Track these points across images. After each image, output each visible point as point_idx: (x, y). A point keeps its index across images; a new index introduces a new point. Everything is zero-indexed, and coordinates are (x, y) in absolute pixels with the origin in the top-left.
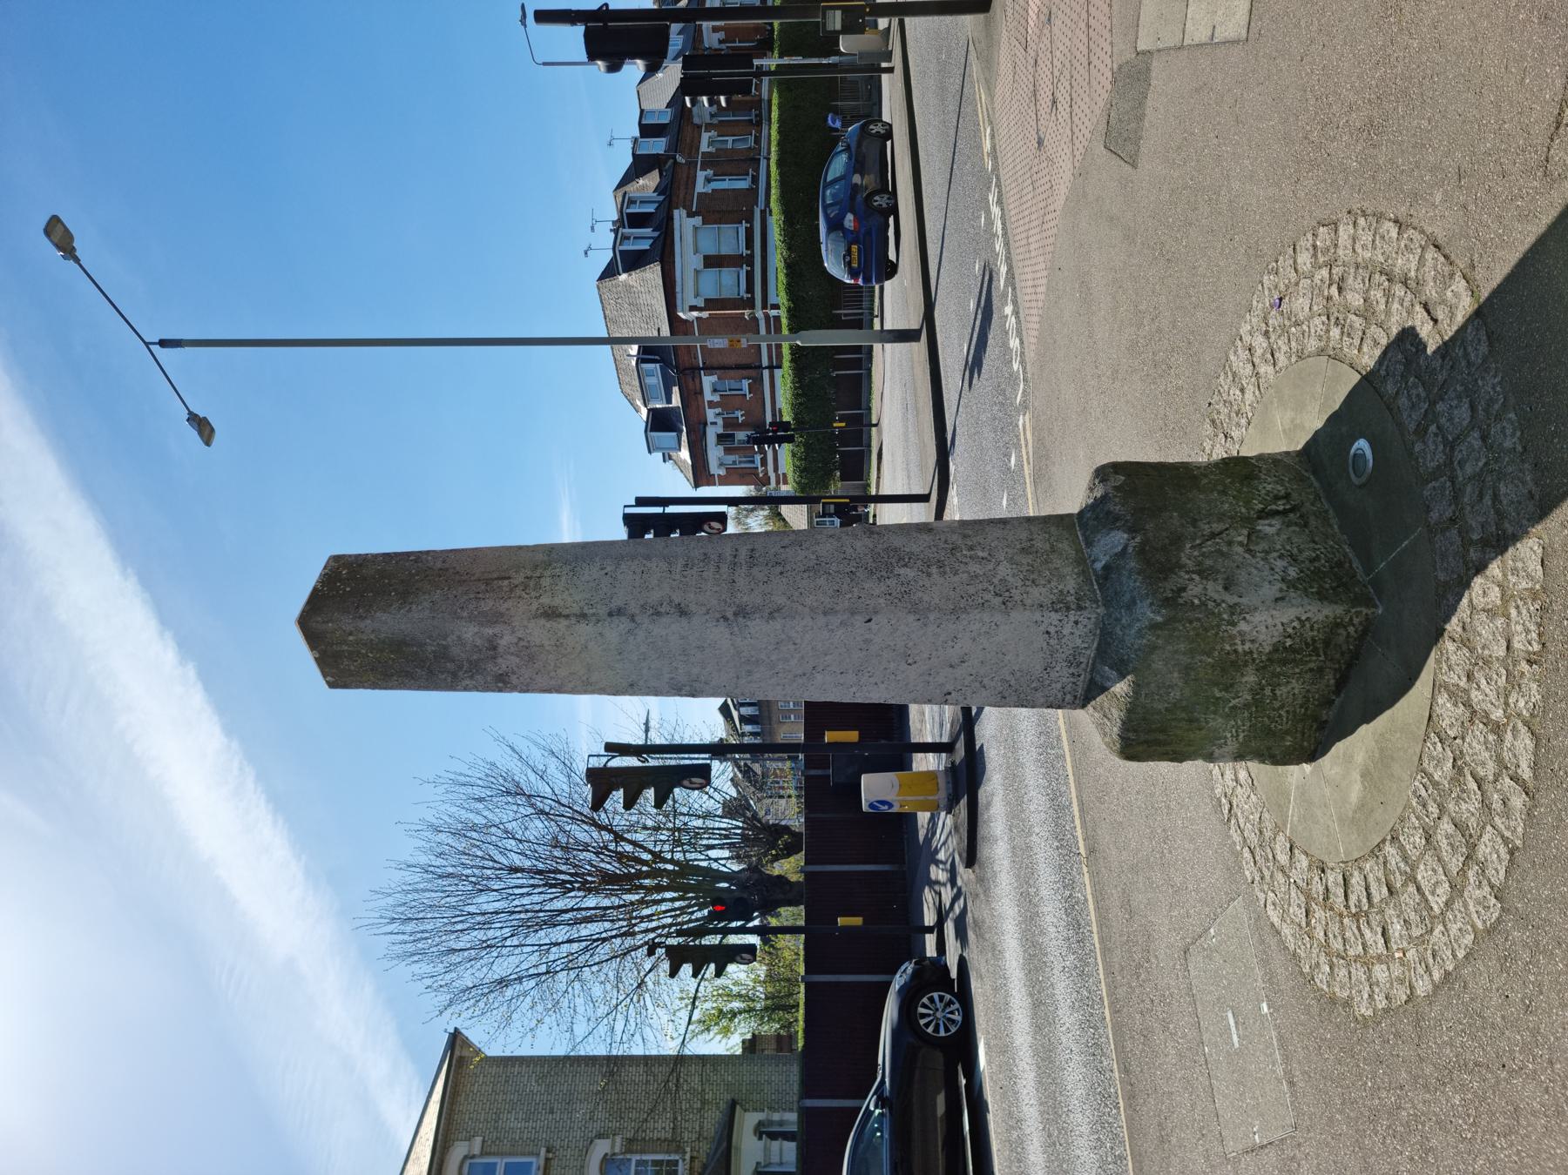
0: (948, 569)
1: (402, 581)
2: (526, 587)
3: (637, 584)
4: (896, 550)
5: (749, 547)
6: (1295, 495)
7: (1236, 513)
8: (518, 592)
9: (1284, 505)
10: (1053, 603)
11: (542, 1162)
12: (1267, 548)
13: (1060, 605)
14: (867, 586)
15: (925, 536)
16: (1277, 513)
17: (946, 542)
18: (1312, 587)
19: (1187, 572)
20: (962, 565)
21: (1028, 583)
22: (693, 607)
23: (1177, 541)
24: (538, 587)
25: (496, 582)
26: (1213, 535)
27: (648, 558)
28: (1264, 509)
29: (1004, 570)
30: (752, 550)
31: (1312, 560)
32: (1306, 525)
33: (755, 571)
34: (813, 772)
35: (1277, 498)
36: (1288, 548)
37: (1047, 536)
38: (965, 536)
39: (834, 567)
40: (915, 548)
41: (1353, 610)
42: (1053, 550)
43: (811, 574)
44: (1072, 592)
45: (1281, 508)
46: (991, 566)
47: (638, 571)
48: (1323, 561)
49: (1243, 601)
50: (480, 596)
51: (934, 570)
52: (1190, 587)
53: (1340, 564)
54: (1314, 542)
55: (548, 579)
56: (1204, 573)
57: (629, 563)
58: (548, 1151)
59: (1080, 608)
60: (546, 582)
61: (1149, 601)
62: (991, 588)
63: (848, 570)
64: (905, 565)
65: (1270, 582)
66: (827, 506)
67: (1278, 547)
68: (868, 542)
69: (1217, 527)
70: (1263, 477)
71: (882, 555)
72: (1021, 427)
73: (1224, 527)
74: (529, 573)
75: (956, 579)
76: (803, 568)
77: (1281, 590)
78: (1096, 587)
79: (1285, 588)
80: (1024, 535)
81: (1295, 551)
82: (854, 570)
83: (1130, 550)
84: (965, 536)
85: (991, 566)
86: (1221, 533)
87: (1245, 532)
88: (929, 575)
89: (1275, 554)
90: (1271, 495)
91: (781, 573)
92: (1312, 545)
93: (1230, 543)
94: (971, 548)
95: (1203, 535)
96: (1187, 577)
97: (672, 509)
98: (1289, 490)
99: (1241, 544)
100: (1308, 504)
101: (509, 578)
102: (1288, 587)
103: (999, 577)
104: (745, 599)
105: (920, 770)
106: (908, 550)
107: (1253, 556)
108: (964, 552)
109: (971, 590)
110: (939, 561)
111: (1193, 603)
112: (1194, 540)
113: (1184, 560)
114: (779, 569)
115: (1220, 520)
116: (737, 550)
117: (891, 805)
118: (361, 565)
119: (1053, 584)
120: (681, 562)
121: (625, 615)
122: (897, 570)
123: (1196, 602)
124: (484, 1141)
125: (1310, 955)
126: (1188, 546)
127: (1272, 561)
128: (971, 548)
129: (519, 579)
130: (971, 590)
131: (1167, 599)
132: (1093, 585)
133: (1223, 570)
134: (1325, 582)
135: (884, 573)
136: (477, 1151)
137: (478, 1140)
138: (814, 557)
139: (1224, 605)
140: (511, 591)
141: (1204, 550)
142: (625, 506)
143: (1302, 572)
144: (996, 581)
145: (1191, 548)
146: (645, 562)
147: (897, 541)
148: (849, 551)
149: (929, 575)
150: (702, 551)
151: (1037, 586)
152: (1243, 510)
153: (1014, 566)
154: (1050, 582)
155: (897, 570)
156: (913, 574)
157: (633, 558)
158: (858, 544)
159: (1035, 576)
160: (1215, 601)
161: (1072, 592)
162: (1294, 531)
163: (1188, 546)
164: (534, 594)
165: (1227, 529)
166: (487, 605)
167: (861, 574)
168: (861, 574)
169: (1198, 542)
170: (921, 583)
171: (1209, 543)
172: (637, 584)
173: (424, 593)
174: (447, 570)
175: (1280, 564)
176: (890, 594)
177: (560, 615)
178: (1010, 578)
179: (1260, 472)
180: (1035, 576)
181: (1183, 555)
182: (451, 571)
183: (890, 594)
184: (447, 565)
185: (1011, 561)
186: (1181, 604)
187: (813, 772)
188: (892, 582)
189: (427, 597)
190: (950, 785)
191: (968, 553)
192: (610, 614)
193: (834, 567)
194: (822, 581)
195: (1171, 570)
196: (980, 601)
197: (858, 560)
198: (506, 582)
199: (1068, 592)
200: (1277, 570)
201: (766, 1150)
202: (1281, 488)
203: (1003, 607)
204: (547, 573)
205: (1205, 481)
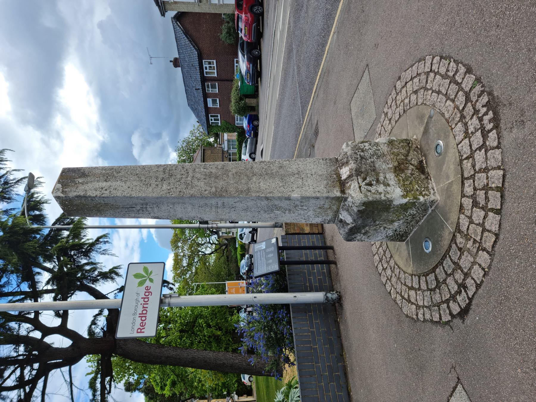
0: (292, 212)
4: (275, 205)
8: (141, 212)
17: (294, 204)
27: (184, 203)
30: (223, 203)
33: (225, 209)
39: (253, 209)
40: (282, 205)
46: (306, 212)
51: (287, 212)
70: (414, 208)
75: (294, 214)
80: (322, 203)
84: (301, 202)
104: (223, 217)
109: (297, 218)
114: (233, 209)
116: (217, 203)
122: (275, 211)
128: (302, 206)
129: (138, 207)
135: (270, 212)
147: (276, 203)
148: (259, 205)
149: (285, 213)
155: (275, 211)
157: (179, 204)
158: (262, 203)
167: (262, 212)
168: (262, 212)
185: (314, 210)
188: (272, 215)
191: (300, 207)
193: (253, 209)
194: (249, 213)
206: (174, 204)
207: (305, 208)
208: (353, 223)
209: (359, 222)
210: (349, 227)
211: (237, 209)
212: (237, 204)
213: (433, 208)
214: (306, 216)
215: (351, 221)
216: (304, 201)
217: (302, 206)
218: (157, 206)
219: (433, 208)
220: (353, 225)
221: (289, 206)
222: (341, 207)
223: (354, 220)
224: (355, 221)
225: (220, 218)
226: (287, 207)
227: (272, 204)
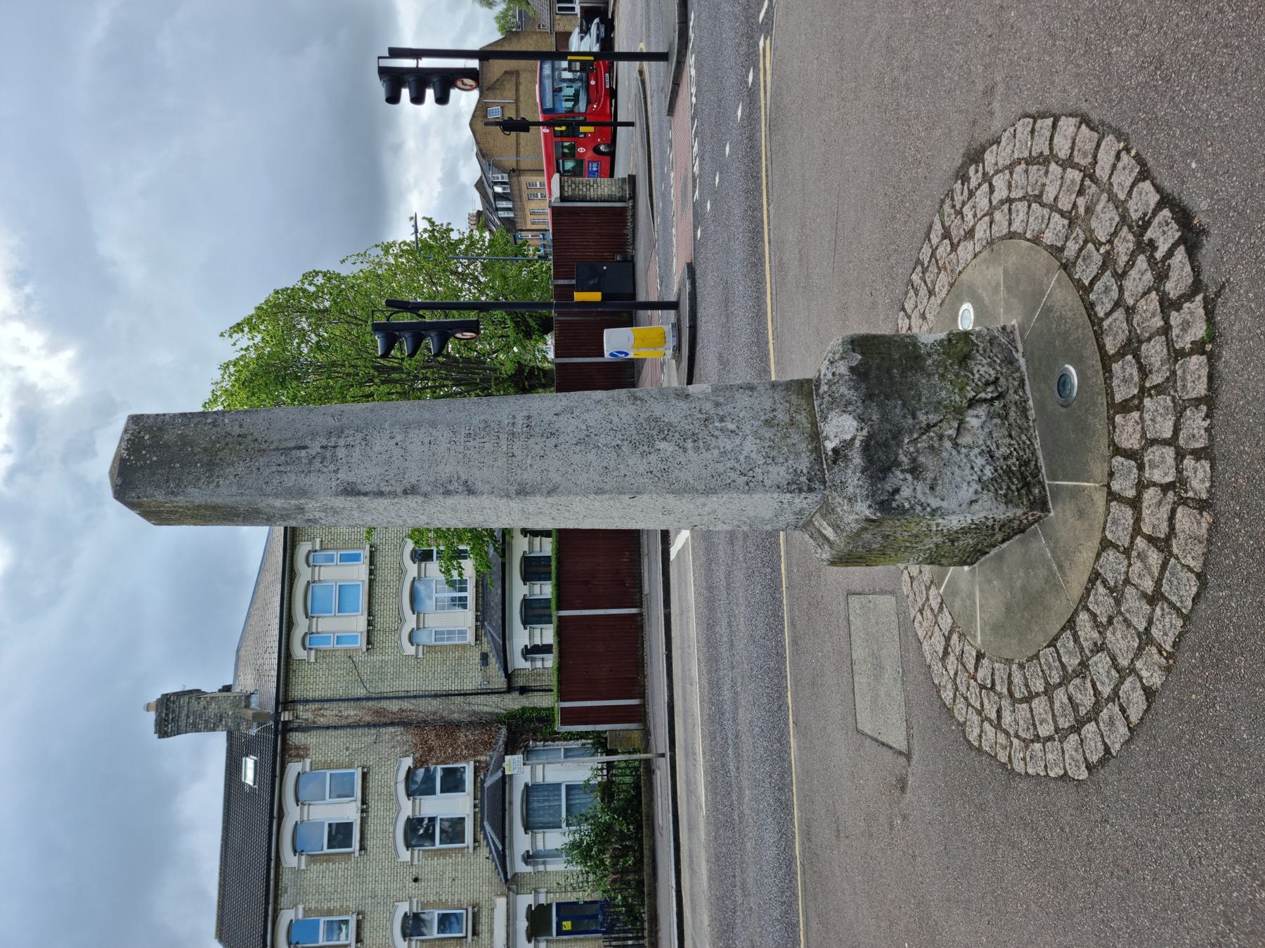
0: (701, 444)
1: (205, 450)
2: (324, 459)
3: (426, 458)
4: (656, 420)
5: (525, 413)
6: (1002, 381)
7: (951, 401)
8: (317, 464)
9: (992, 392)
10: (789, 483)
11: (368, 554)
12: (971, 443)
13: (793, 486)
14: (631, 462)
15: (682, 404)
16: (985, 400)
18: (1001, 489)
19: (903, 471)
20: (714, 439)
21: (769, 461)
22: (480, 486)
23: (897, 435)
24: (335, 459)
25: (294, 452)
26: (929, 427)
27: (433, 425)
28: (975, 396)
29: (750, 445)
30: (529, 417)
31: (1006, 458)
32: (1006, 417)
34: (561, 282)
35: (987, 384)
36: (989, 443)
37: (787, 405)
38: (717, 404)
39: (602, 440)
41: (1030, 514)
42: (792, 423)
43: (583, 448)
44: (805, 471)
45: (989, 396)
47: (426, 441)
48: (1015, 460)
49: (944, 504)
50: (282, 468)
51: (689, 444)
52: (904, 488)
53: (1027, 463)
54: (1010, 436)
55: (343, 450)
56: (915, 470)
57: (416, 431)
58: (371, 547)
59: (810, 490)
60: (341, 453)
61: (868, 503)
62: (737, 466)
63: (614, 443)
64: (664, 439)
65: (969, 483)
66: (573, 64)
67: (981, 442)
68: (631, 409)
69: (933, 418)
70: (979, 357)
71: (644, 425)
72: (761, 48)
73: (940, 419)
74: (325, 442)
76: (574, 441)
77: (976, 492)
78: (825, 467)
79: (980, 490)
80: (768, 404)
81: (993, 447)
82: (619, 442)
83: (857, 443)
84: (717, 404)
85: (738, 442)
86: (935, 425)
87: (955, 424)
88: (685, 450)
89: (977, 451)
90: (983, 380)
91: (556, 446)
92: (1008, 440)
93: (941, 437)
94: (722, 420)
95: (920, 428)
96: (902, 477)
97: (426, 63)
98: (999, 375)
99: (950, 437)
100: (1011, 391)
101: (305, 447)
102: (983, 489)
103: (745, 453)
104: (525, 476)
105: (650, 300)
106: (666, 420)
107: (959, 452)
108: (717, 424)
109: (721, 467)
110: (694, 434)
111: (904, 506)
112: (911, 433)
113: (903, 458)
114: (553, 441)
115: (936, 410)
117: (627, 354)
118: (160, 429)
119: (791, 462)
120: (463, 432)
121: (418, 493)
123: (907, 505)
124: (321, 541)
125: (941, 677)
126: (906, 441)
127: (973, 458)
129: (315, 448)
130: (721, 467)
131: (882, 503)
132: (822, 464)
133: (933, 468)
134: (1013, 483)
135: (645, 448)
136: (318, 547)
137: (318, 541)
138: (584, 427)
139: (928, 509)
140: (310, 463)
141: (919, 445)
142: (379, 58)
143: (996, 470)
144: (742, 458)
145: (908, 443)
146: (431, 429)
148: (615, 420)
149: (685, 450)
150: (482, 417)
151: (776, 464)
152: (958, 399)
153: (758, 441)
154: (787, 460)
156: (671, 449)
158: (623, 412)
159: (774, 453)
160: (922, 505)
161: (805, 471)
162: (996, 425)
163: (906, 441)
164: (332, 467)
165: (941, 421)
166: (290, 480)
167: (626, 448)
169: (915, 436)
170: (678, 461)
171: (924, 437)
172: (426, 458)
173: (228, 465)
174: (244, 436)
175: (980, 461)
176: (651, 472)
177: (359, 493)
178: (754, 455)
179: (978, 351)
180: (774, 453)
181: (901, 451)
182: (250, 437)
183: (651, 472)
184: (244, 431)
185: (756, 434)
186: (894, 509)
187: (561, 282)
188: (653, 458)
189: (231, 469)
190: (675, 338)
191: (717, 424)
192: (405, 492)
193: (602, 440)
194: (591, 456)
195: (889, 469)
196: (729, 481)
197: (623, 432)
198: (303, 453)
199: (802, 472)
200: (976, 469)
201: (531, 544)
202: (992, 372)
203: (747, 488)
204: (342, 442)
205: (929, 362)
206: (407, 427)
207: (731, 426)
208: (862, 429)
209: (874, 417)
210: (857, 443)
211: (561, 439)
212: (561, 422)
213: (1021, 350)
214: (742, 458)
215: (855, 424)
216: (722, 400)
217: (722, 420)
218: (365, 439)
219: (1021, 350)
220: (865, 432)
221: (690, 420)
222: (818, 419)
223: (861, 419)
224: (863, 420)
225: (518, 478)
226: (685, 425)
227: (648, 414)
